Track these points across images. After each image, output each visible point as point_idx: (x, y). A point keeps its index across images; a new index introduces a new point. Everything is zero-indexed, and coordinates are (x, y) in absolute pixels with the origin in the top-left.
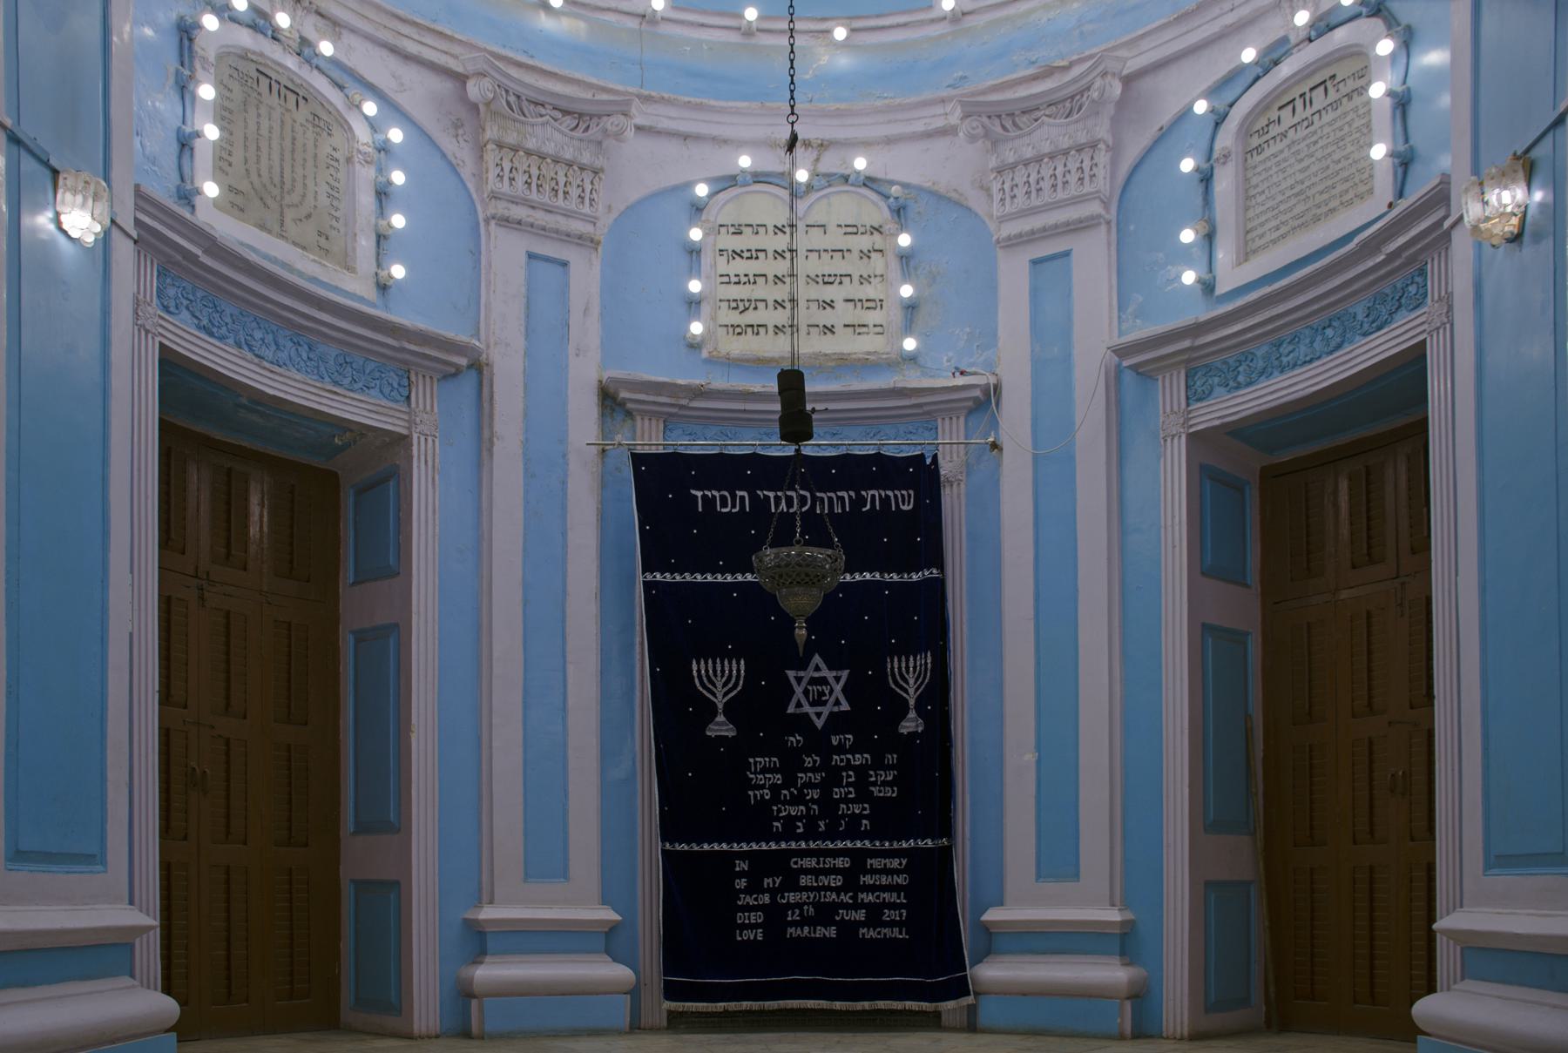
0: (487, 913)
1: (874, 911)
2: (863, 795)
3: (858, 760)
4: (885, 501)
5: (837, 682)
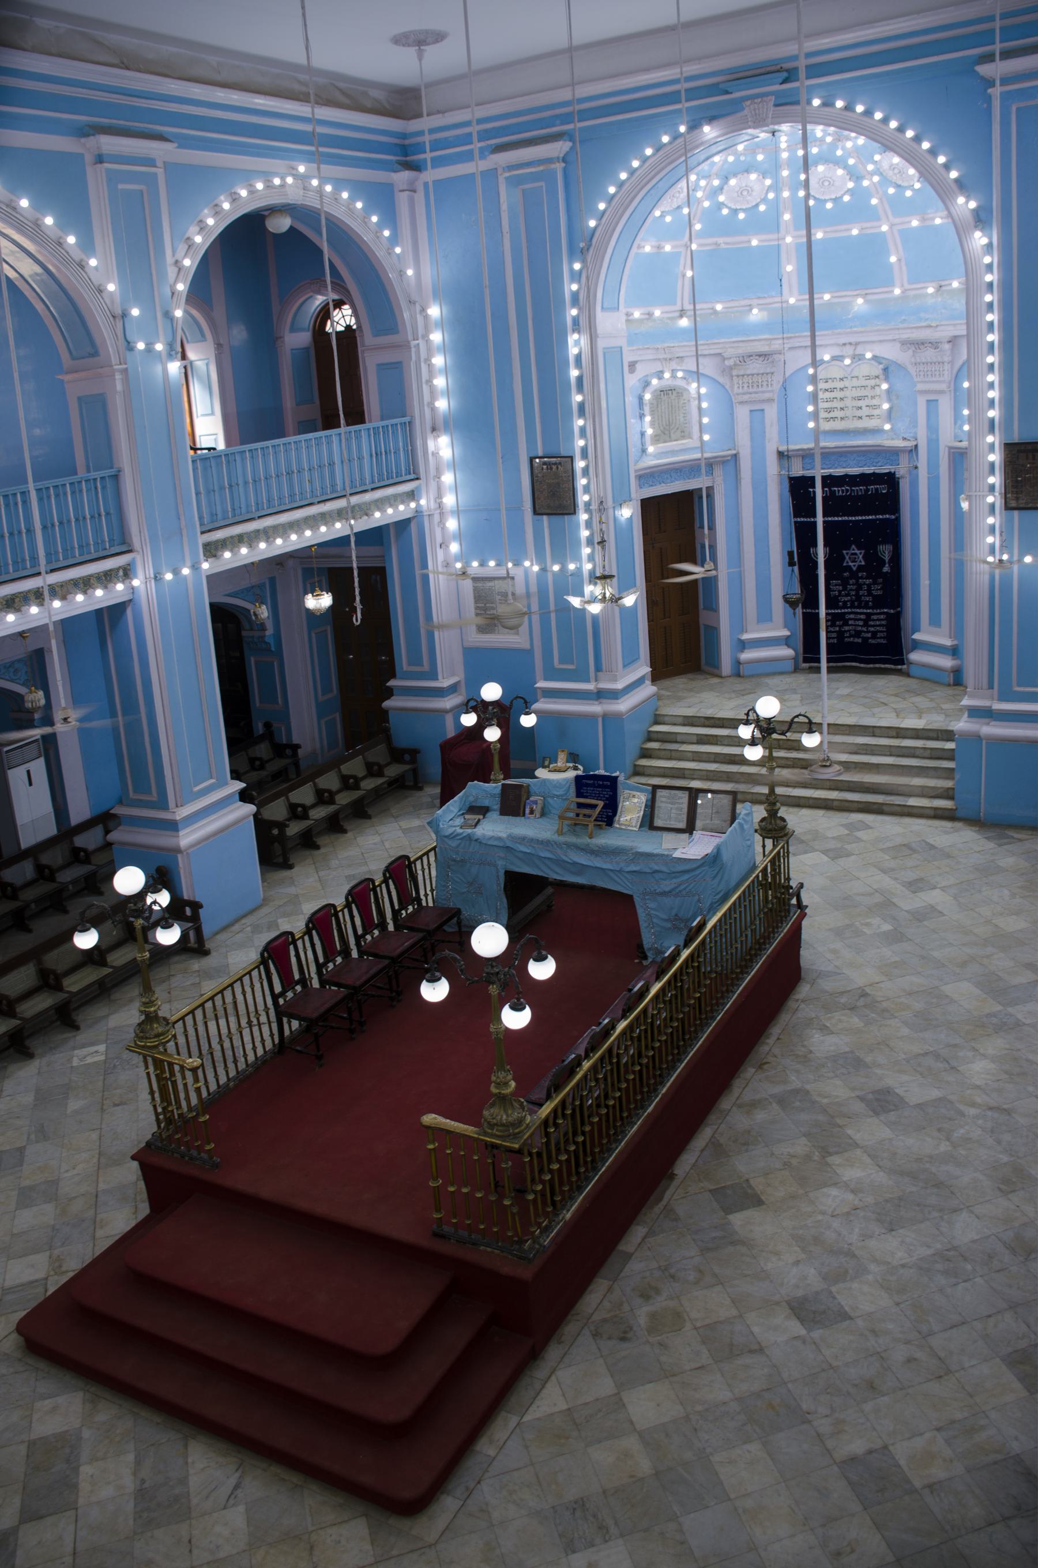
0: (745, 637)
1: (874, 635)
2: (870, 594)
3: (868, 581)
5: (860, 554)
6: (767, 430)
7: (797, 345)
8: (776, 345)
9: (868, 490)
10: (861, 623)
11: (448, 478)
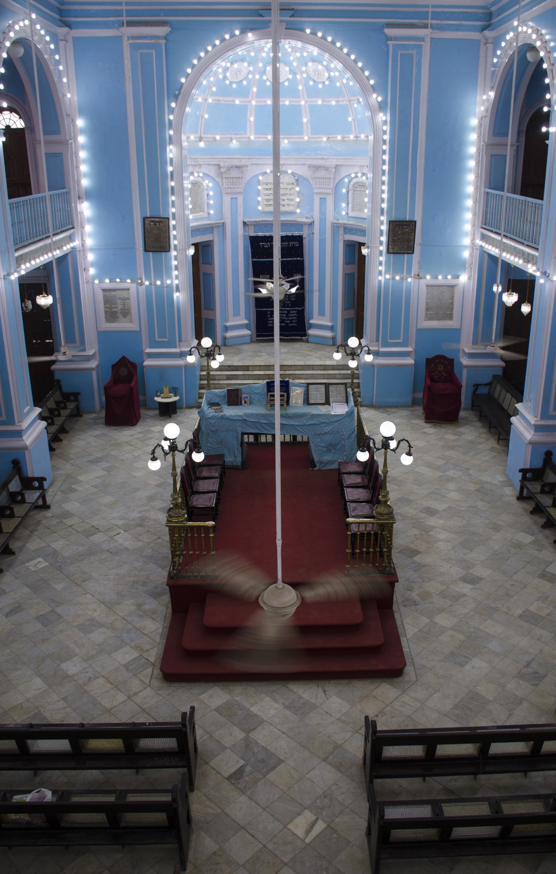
0: (228, 324)
1: (291, 321)
4: (293, 244)
6: (239, 209)
7: (254, 163)
8: (243, 162)
9: (289, 244)
10: (285, 315)
11: (88, 228)
